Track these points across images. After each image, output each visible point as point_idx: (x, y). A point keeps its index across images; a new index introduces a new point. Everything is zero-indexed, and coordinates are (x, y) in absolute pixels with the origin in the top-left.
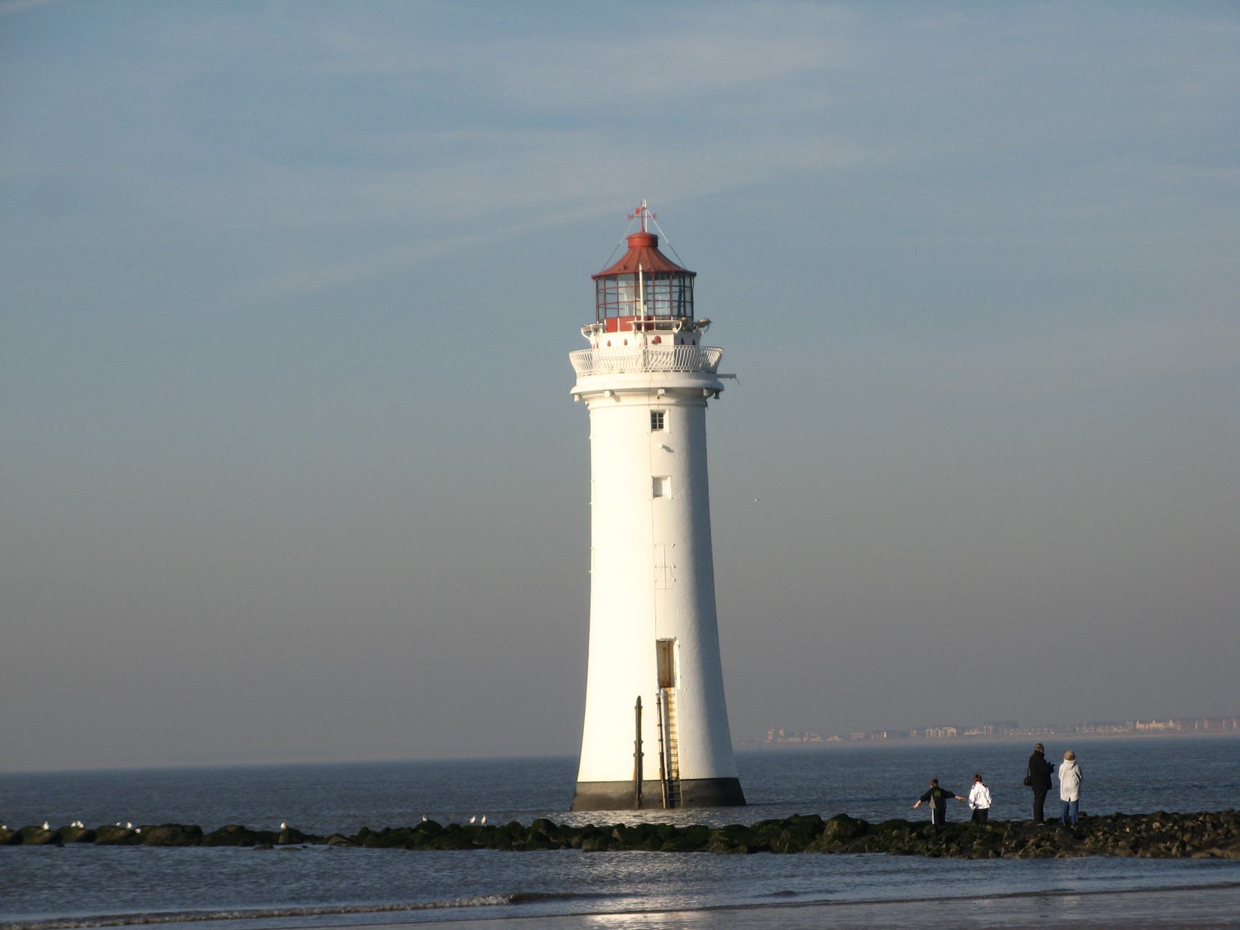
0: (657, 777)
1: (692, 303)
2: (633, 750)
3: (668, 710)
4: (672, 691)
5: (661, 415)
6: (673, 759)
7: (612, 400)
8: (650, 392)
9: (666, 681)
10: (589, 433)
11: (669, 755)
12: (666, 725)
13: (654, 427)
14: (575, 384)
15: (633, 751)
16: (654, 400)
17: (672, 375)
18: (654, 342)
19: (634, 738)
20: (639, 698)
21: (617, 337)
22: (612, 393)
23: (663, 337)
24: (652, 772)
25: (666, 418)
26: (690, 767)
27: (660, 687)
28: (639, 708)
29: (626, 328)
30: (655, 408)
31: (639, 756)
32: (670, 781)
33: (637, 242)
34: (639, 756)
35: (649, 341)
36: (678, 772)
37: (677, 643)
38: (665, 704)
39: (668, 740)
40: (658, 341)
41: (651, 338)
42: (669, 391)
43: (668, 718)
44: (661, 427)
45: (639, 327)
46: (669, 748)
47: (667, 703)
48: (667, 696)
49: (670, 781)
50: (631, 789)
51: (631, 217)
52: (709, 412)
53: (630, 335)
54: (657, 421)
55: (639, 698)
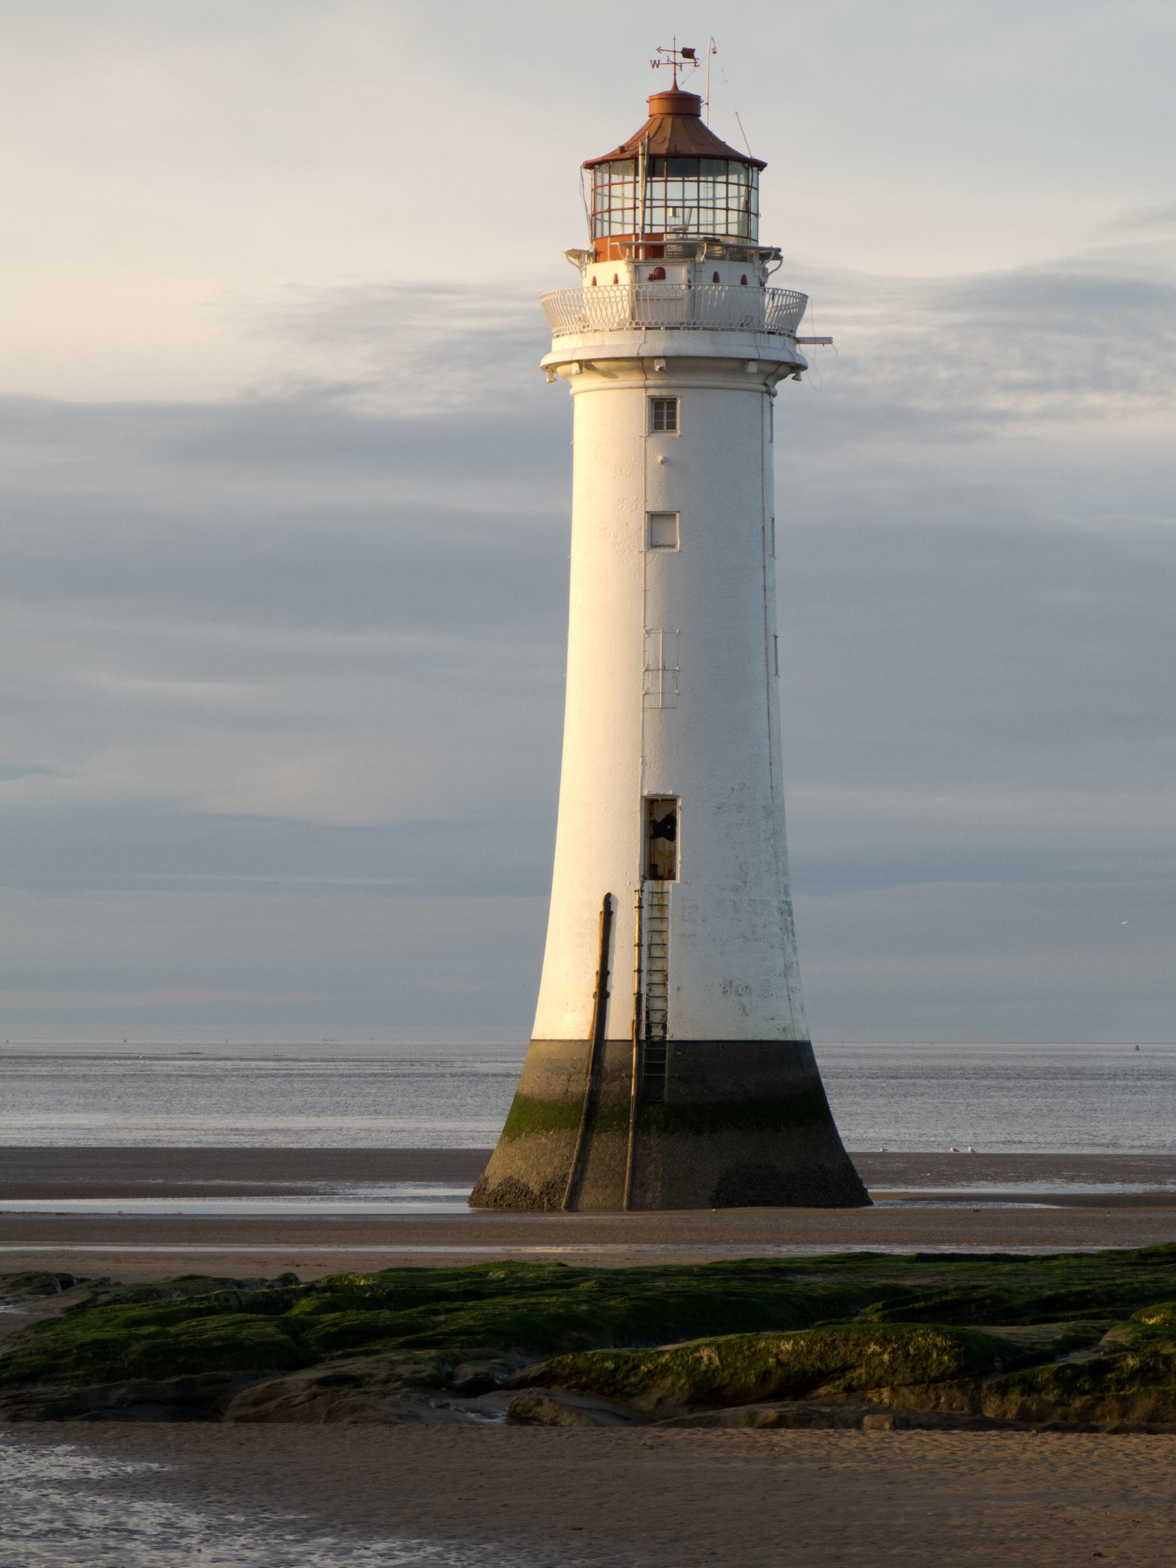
2: (591, 983)
4: (669, 885)
5: (672, 403)
8: (640, 363)
14: (548, 349)
19: (596, 967)
23: (669, 270)
24: (620, 1027)
34: (602, 996)
44: (672, 426)
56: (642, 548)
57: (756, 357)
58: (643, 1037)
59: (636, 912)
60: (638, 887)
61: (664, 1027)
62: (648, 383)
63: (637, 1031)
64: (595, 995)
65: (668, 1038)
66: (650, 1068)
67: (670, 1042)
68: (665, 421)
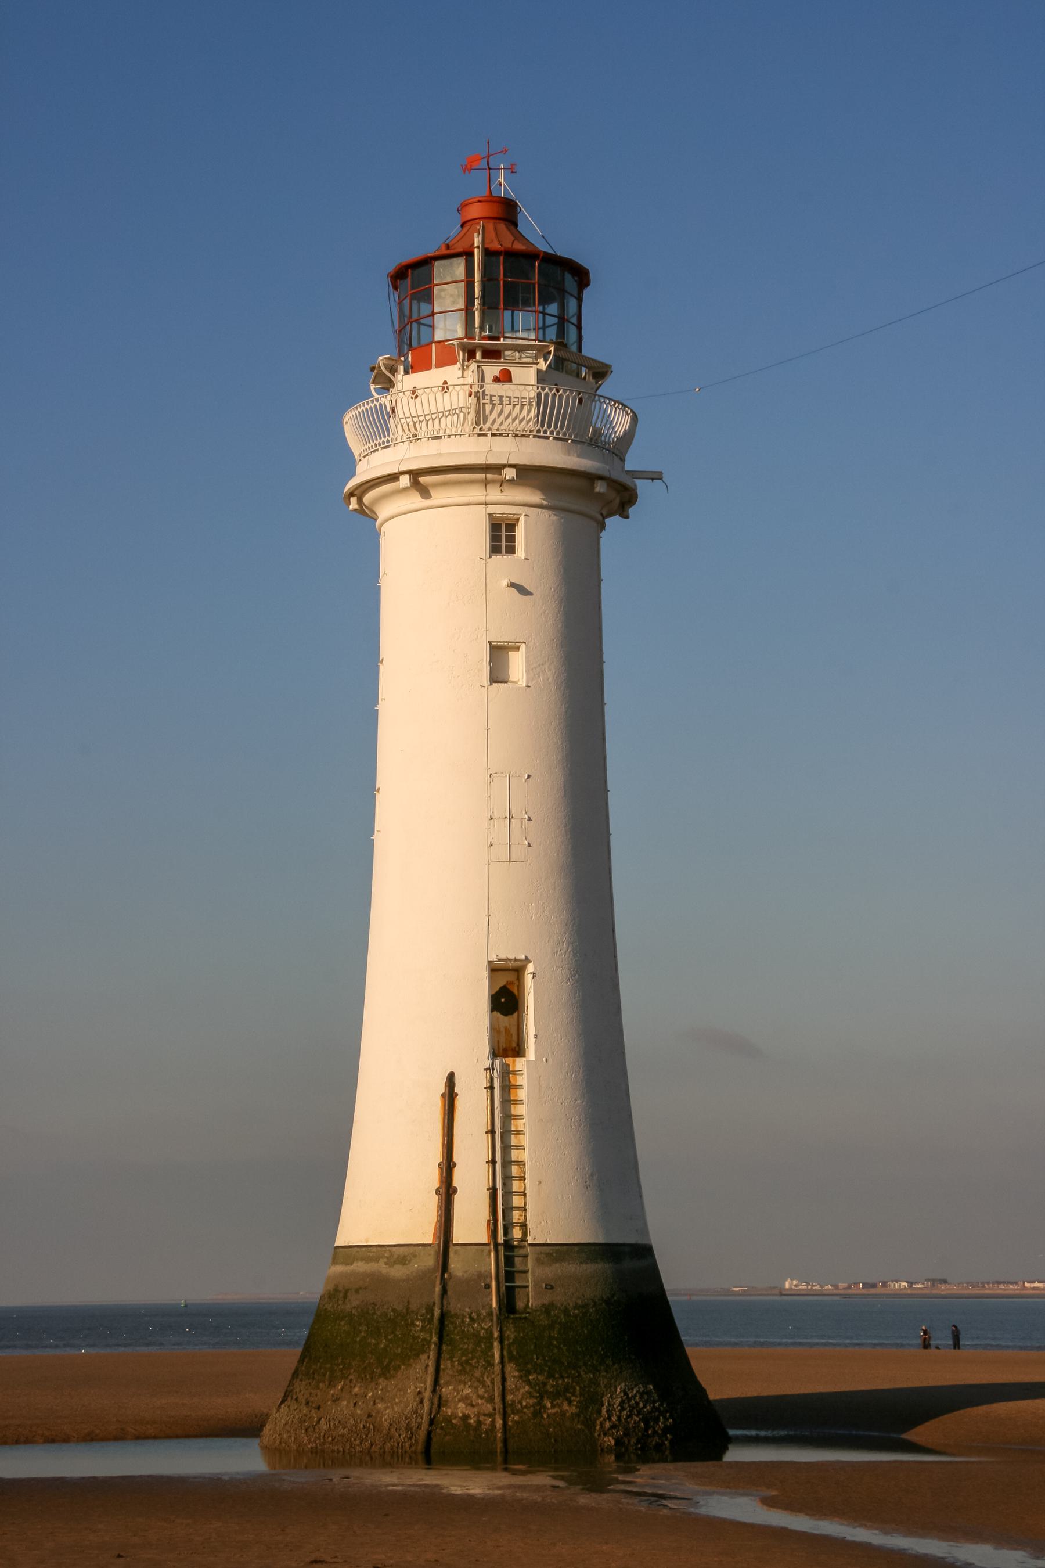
0: (483, 1237)
1: (579, 328)
2: (434, 1179)
3: (507, 1102)
4: (519, 1063)
5: (511, 527)
6: (517, 1201)
7: (415, 500)
9: (507, 1046)
11: (508, 1194)
12: (502, 1131)
13: (495, 550)
15: (435, 1183)
16: (494, 494)
18: (496, 380)
19: (437, 1156)
20: (451, 1079)
22: (415, 475)
23: (515, 371)
24: (471, 1225)
25: (520, 532)
27: (495, 1054)
28: (450, 1097)
30: (498, 510)
31: (447, 1192)
34: (447, 1192)
35: (489, 378)
36: (524, 1226)
37: (530, 968)
38: (503, 1090)
39: (507, 1163)
40: (505, 377)
42: (527, 474)
43: (508, 1117)
44: (511, 550)
45: (471, 355)
46: (507, 1178)
47: (508, 1087)
48: (507, 1073)
49: (508, 1245)
50: (429, 1261)
51: (468, 168)
52: (606, 537)
53: (452, 373)
54: (501, 536)
55: (451, 1079)
56: (484, 683)
57: (606, 474)
58: (501, 1239)
59: (484, 1094)
60: (487, 1064)
62: (489, 499)
63: (494, 1233)
64: (437, 1192)
66: (510, 1276)
67: (531, 1245)
68: (504, 544)
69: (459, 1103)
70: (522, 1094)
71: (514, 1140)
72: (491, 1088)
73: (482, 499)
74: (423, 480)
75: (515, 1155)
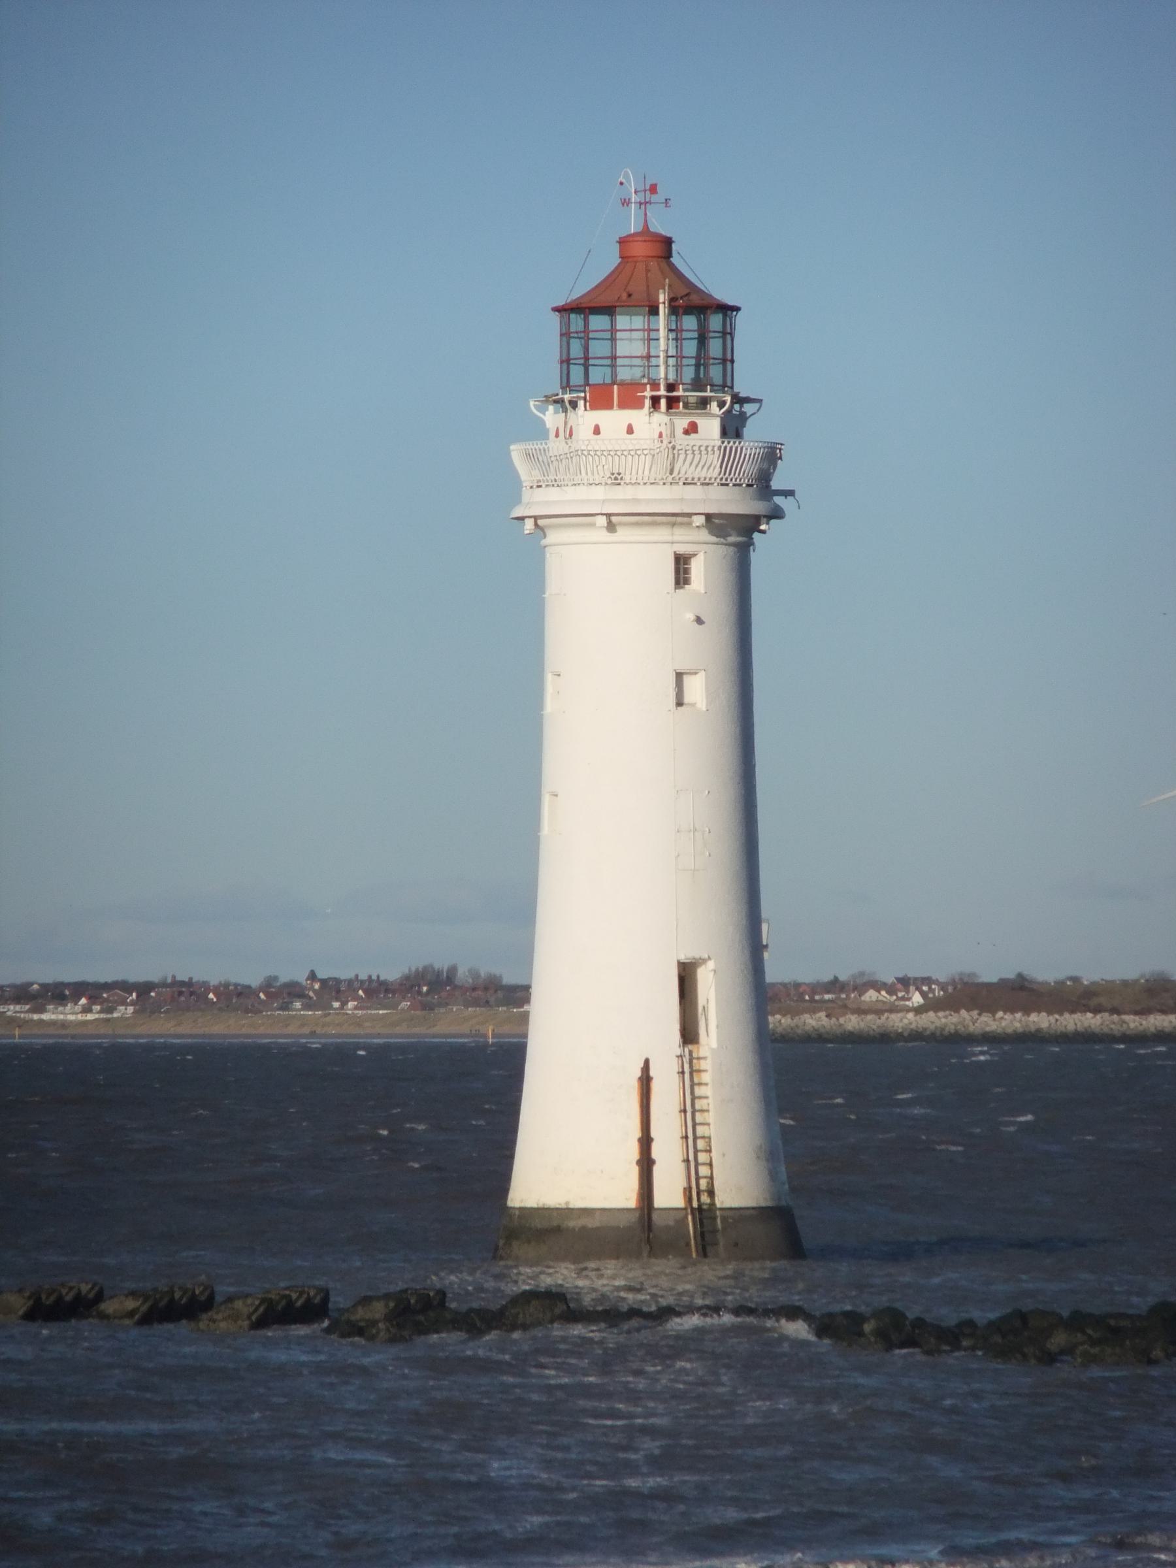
0: (679, 1202)
2: (634, 1152)
7: (604, 535)
10: (542, 589)
12: (690, 1109)
16: (680, 534)
17: (716, 492)
18: (686, 432)
19: (637, 1133)
20: (647, 1062)
21: (613, 420)
23: (701, 422)
24: (669, 1193)
26: (738, 1185)
28: (645, 1081)
29: (630, 401)
30: (682, 549)
31: (646, 1164)
32: (700, 1209)
33: (640, 249)
34: (646, 1164)
38: (690, 1072)
40: (692, 429)
41: (682, 423)
44: (687, 581)
49: (700, 1209)
55: (647, 1062)
58: (695, 1204)
61: (711, 1193)
62: (676, 538)
63: (689, 1199)
64: (638, 1163)
65: (718, 1205)
67: (721, 1209)
69: (655, 1086)
70: (706, 1077)
71: (699, 1118)
72: (683, 1073)
73: (669, 538)
74: (614, 519)
75: (700, 1130)
